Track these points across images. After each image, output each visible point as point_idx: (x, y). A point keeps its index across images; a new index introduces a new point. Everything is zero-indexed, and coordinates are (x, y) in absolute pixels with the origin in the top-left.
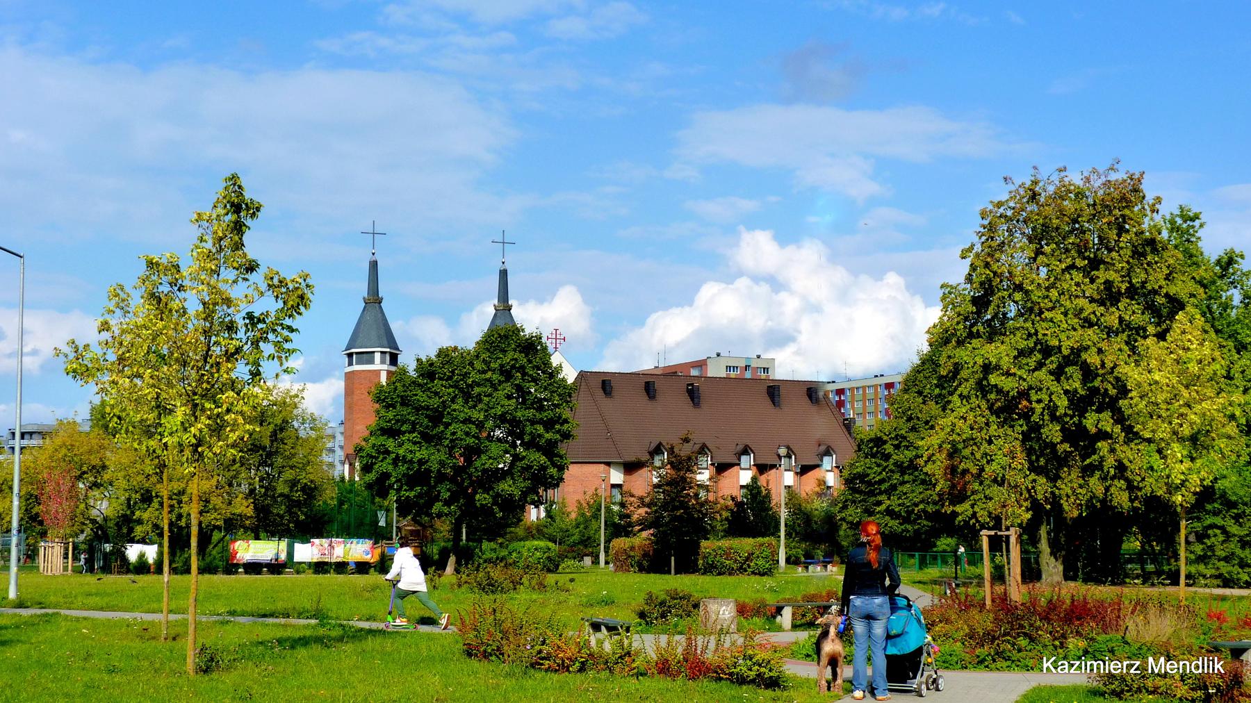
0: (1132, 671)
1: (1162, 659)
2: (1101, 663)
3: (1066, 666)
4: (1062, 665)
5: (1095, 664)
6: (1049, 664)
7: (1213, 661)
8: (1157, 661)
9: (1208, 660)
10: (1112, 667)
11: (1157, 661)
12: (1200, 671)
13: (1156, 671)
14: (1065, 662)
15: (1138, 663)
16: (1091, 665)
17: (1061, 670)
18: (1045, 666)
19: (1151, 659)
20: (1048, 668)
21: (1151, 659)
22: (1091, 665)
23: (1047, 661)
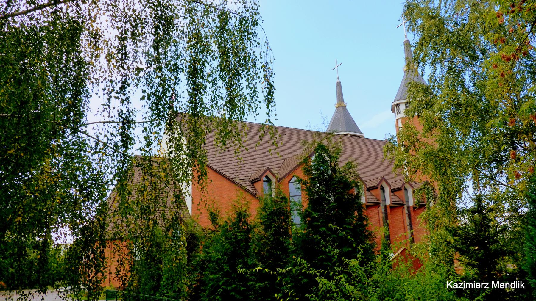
0: (485, 287)
1: (498, 282)
2: (472, 284)
3: (457, 285)
4: (456, 284)
5: (469, 284)
6: (449, 284)
7: (520, 283)
8: (496, 283)
9: (518, 283)
10: (476, 285)
11: (496, 283)
12: (514, 287)
13: (495, 287)
14: (457, 284)
15: (488, 284)
16: (468, 285)
17: (455, 287)
18: (448, 285)
19: (493, 282)
20: (449, 286)
21: (493, 282)
22: (468, 285)
23: (449, 282)
